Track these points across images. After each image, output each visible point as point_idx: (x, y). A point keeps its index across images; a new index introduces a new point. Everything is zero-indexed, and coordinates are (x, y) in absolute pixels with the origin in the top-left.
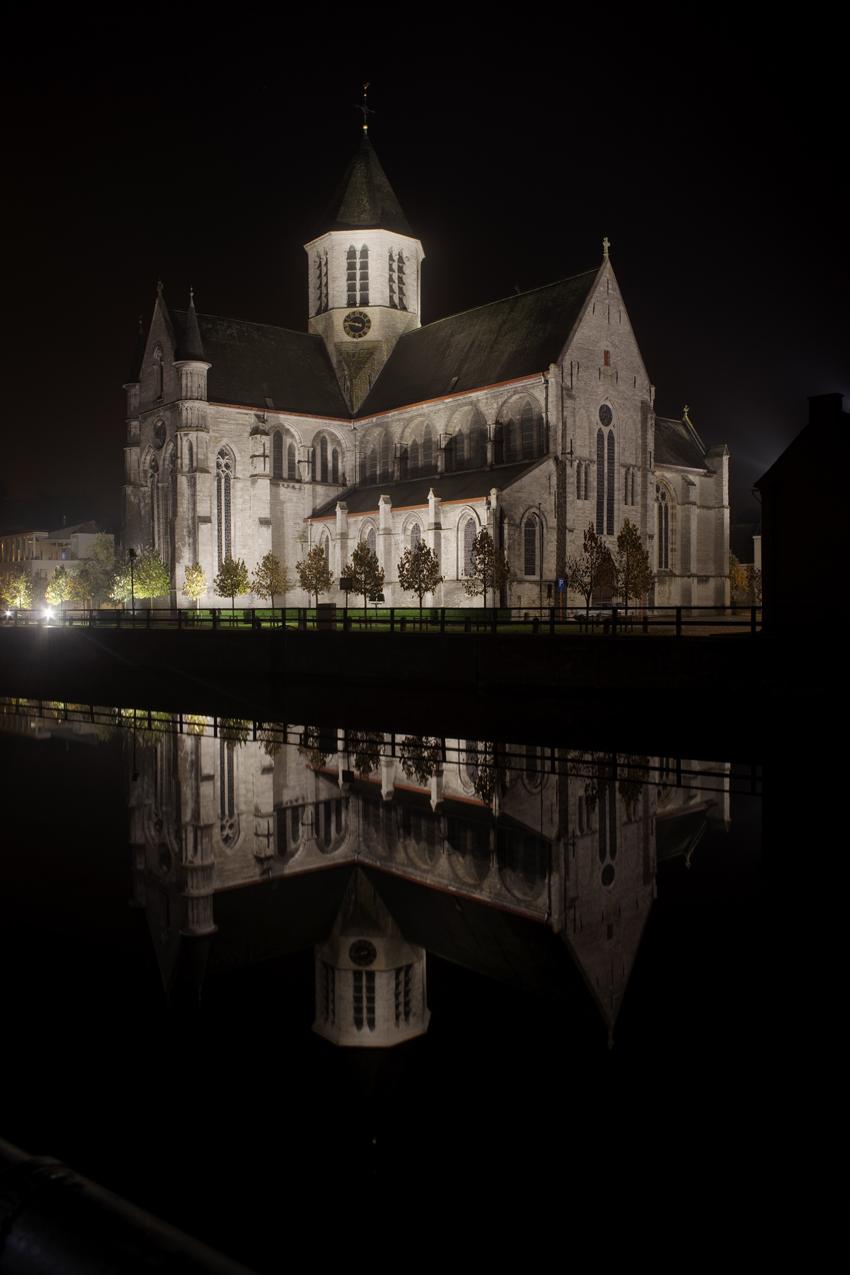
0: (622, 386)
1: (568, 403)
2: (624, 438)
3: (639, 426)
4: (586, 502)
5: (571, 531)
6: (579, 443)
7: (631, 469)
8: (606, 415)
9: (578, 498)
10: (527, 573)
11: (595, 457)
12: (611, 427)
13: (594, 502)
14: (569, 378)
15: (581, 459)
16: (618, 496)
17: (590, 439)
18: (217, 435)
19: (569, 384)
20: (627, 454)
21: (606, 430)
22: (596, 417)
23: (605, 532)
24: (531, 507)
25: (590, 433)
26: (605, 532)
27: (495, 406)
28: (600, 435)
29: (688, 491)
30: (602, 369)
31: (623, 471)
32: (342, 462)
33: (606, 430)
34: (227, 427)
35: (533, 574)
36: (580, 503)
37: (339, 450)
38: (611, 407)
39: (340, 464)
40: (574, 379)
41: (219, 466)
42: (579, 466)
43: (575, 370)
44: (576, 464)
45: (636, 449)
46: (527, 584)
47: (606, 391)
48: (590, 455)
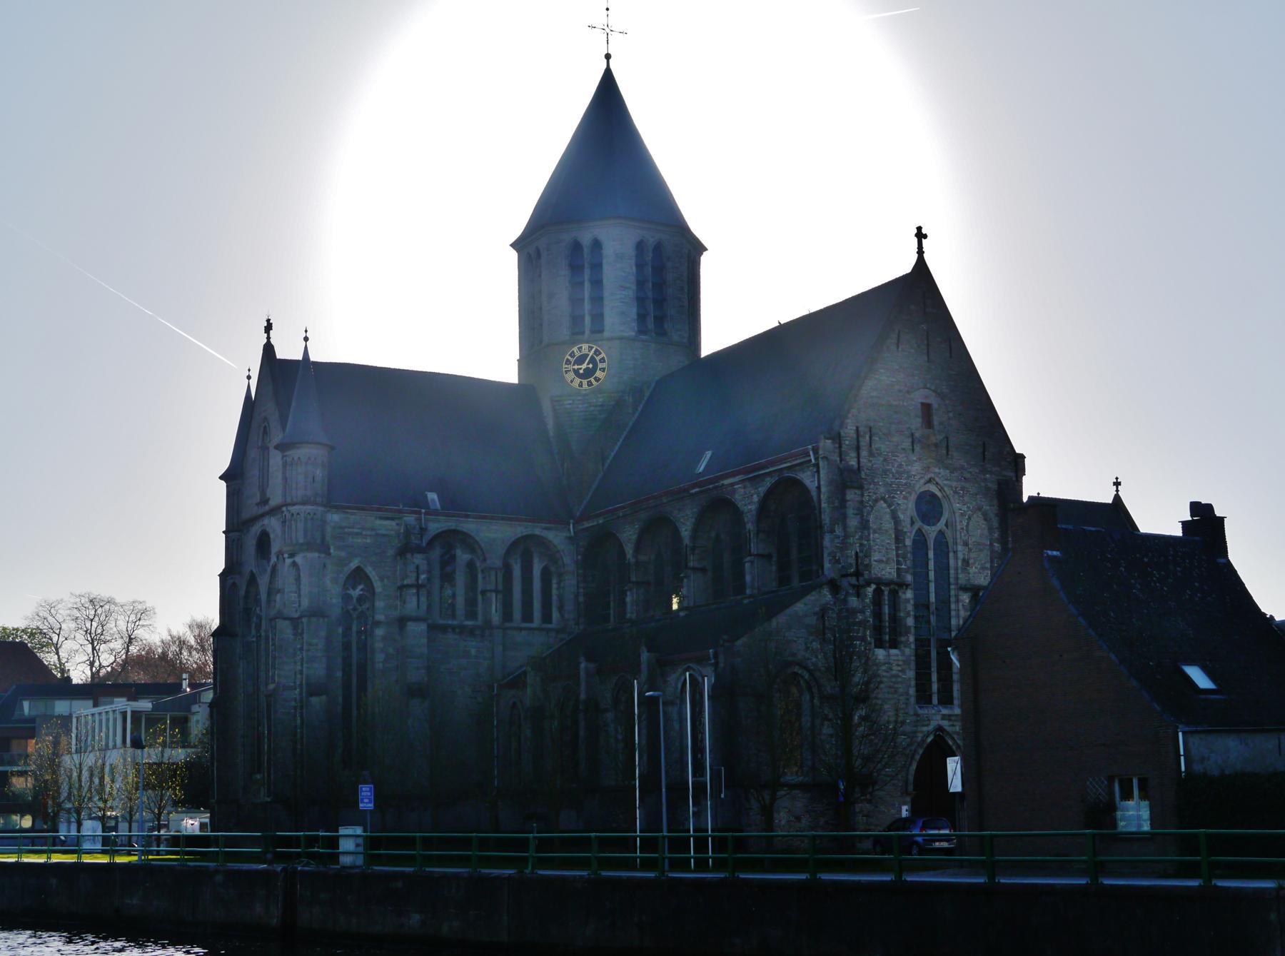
1: (851, 495)
2: (966, 544)
3: (995, 524)
4: (893, 651)
9: (880, 644)
11: (909, 578)
12: (943, 521)
13: (909, 651)
14: (853, 454)
15: (879, 582)
17: (897, 548)
18: (343, 554)
19: (853, 463)
20: (973, 570)
21: (931, 532)
22: (907, 508)
23: (935, 700)
25: (899, 537)
26: (935, 700)
27: (755, 498)
28: (920, 541)
30: (917, 435)
31: (965, 598)
32: (558, 588)
34: (359, 540)
36: (881, 653)
37: (553, 569)
38: (939, 494)
39: (554, 592)
40: (864, 453)
41: (346, 598)
42: (878, 592)
43: (864, 441)
44: (870, 590)
45: (992, 561)
47: (927, 469)
48: (899, 575)
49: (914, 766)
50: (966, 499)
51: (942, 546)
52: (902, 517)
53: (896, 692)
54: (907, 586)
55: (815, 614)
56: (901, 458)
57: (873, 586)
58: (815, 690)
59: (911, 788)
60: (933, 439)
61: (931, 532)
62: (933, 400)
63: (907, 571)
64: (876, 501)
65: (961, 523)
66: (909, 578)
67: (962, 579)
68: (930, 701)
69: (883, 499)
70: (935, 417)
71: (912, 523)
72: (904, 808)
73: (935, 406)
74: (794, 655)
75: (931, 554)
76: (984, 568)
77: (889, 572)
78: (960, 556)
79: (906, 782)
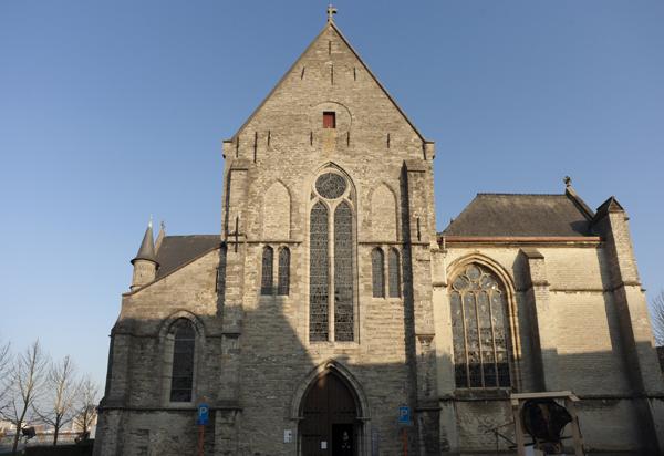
0: (360, 147)
2: (368, 209)
5: (234, 336)
6: (268, 223)
7: (384, 248)
8: (332, 184)
10: (175, 395)
12: (345, 196)
16: (364, 283)
22: (306, 188)
23: (332, 336)
24: (179, 310)
26: (332, 336)
28: (319, 214)
29: (527, 268)
31: (365, 251)
33: (332, 205)
35: (189, 400)
38: (341, 174)
42: (269, 249)
44: (259, 249)
46: (163, 414)
49: (300, 394)
50: (367, 175)
51: (346, 215)
52: (296, 191)
53: (281, 330)
54: (299, 243)
55: (208, 271)
56: (299, 150)
57: (262, 245)
58: (202, 331)
59: (295, 415)
60: (335, 135)
61: (332, 205)
62: (335, 108)
63: (300, 232)
64: (271, 182)
65: (362, 193)
66: (300, 238)
67: (362, 236)
68: (326, 337)
69: (279, 180)
70: (337, 120)
71: (313, 196)
72: (287, 432)
73: (338, 113)
74: (184, 303)
75: (332, 219)
76: (389, 227)
77: (283, 235)
78: (360, 219)
79: (289, 407)
